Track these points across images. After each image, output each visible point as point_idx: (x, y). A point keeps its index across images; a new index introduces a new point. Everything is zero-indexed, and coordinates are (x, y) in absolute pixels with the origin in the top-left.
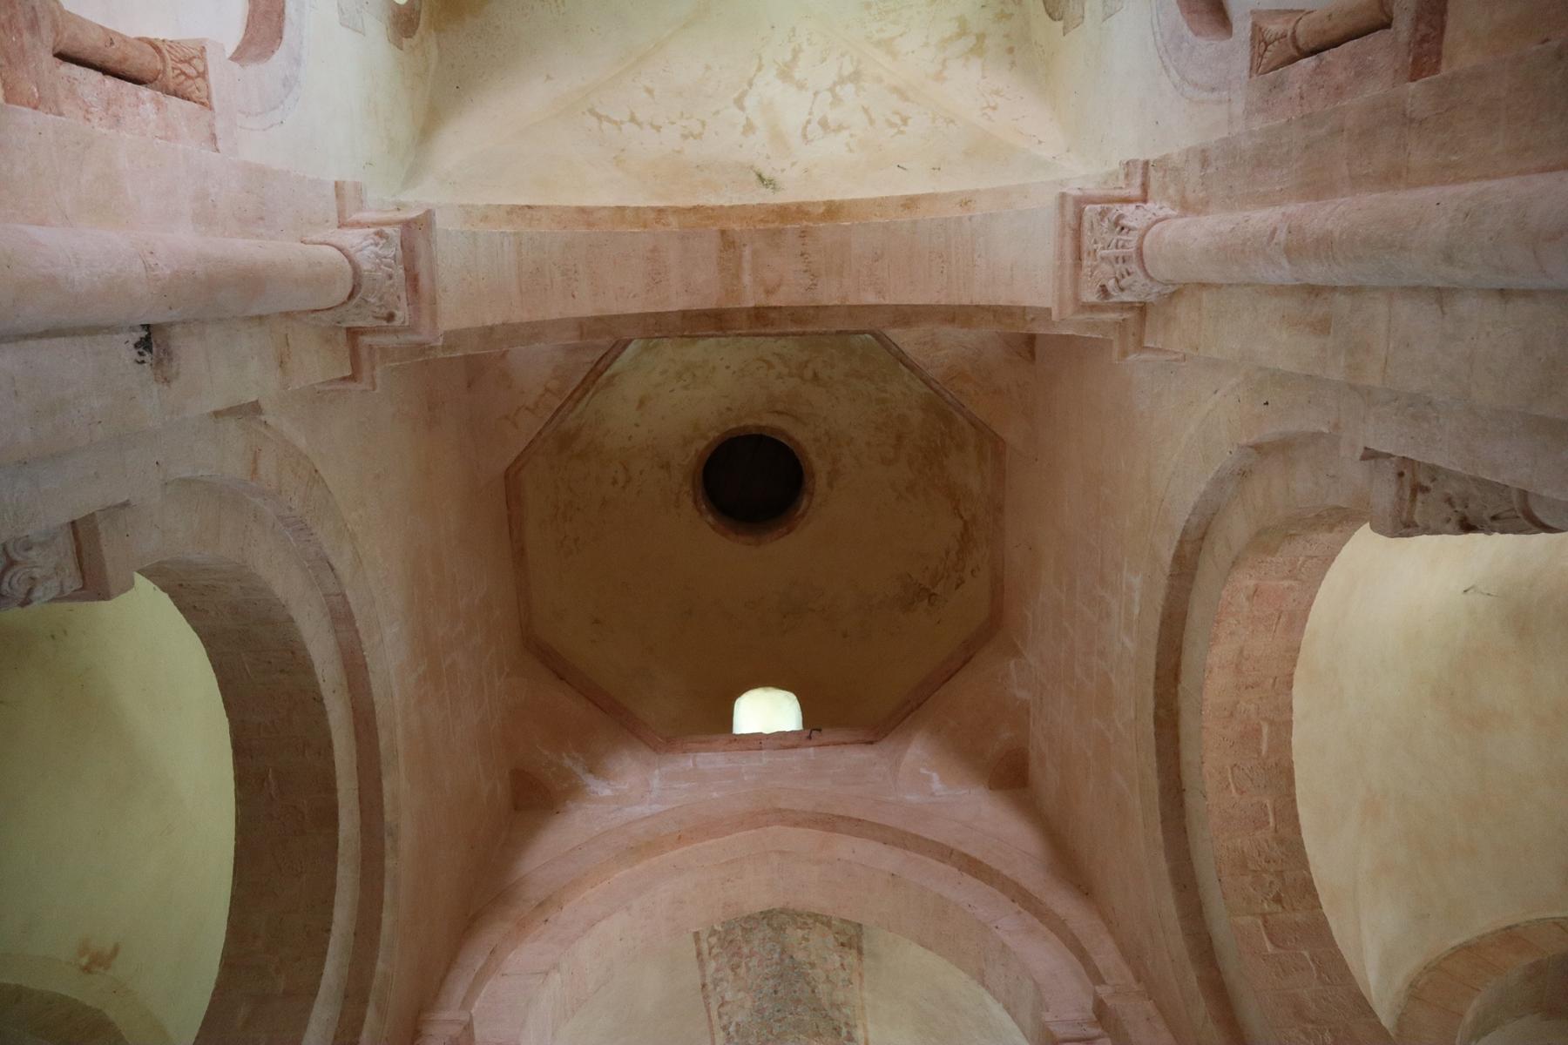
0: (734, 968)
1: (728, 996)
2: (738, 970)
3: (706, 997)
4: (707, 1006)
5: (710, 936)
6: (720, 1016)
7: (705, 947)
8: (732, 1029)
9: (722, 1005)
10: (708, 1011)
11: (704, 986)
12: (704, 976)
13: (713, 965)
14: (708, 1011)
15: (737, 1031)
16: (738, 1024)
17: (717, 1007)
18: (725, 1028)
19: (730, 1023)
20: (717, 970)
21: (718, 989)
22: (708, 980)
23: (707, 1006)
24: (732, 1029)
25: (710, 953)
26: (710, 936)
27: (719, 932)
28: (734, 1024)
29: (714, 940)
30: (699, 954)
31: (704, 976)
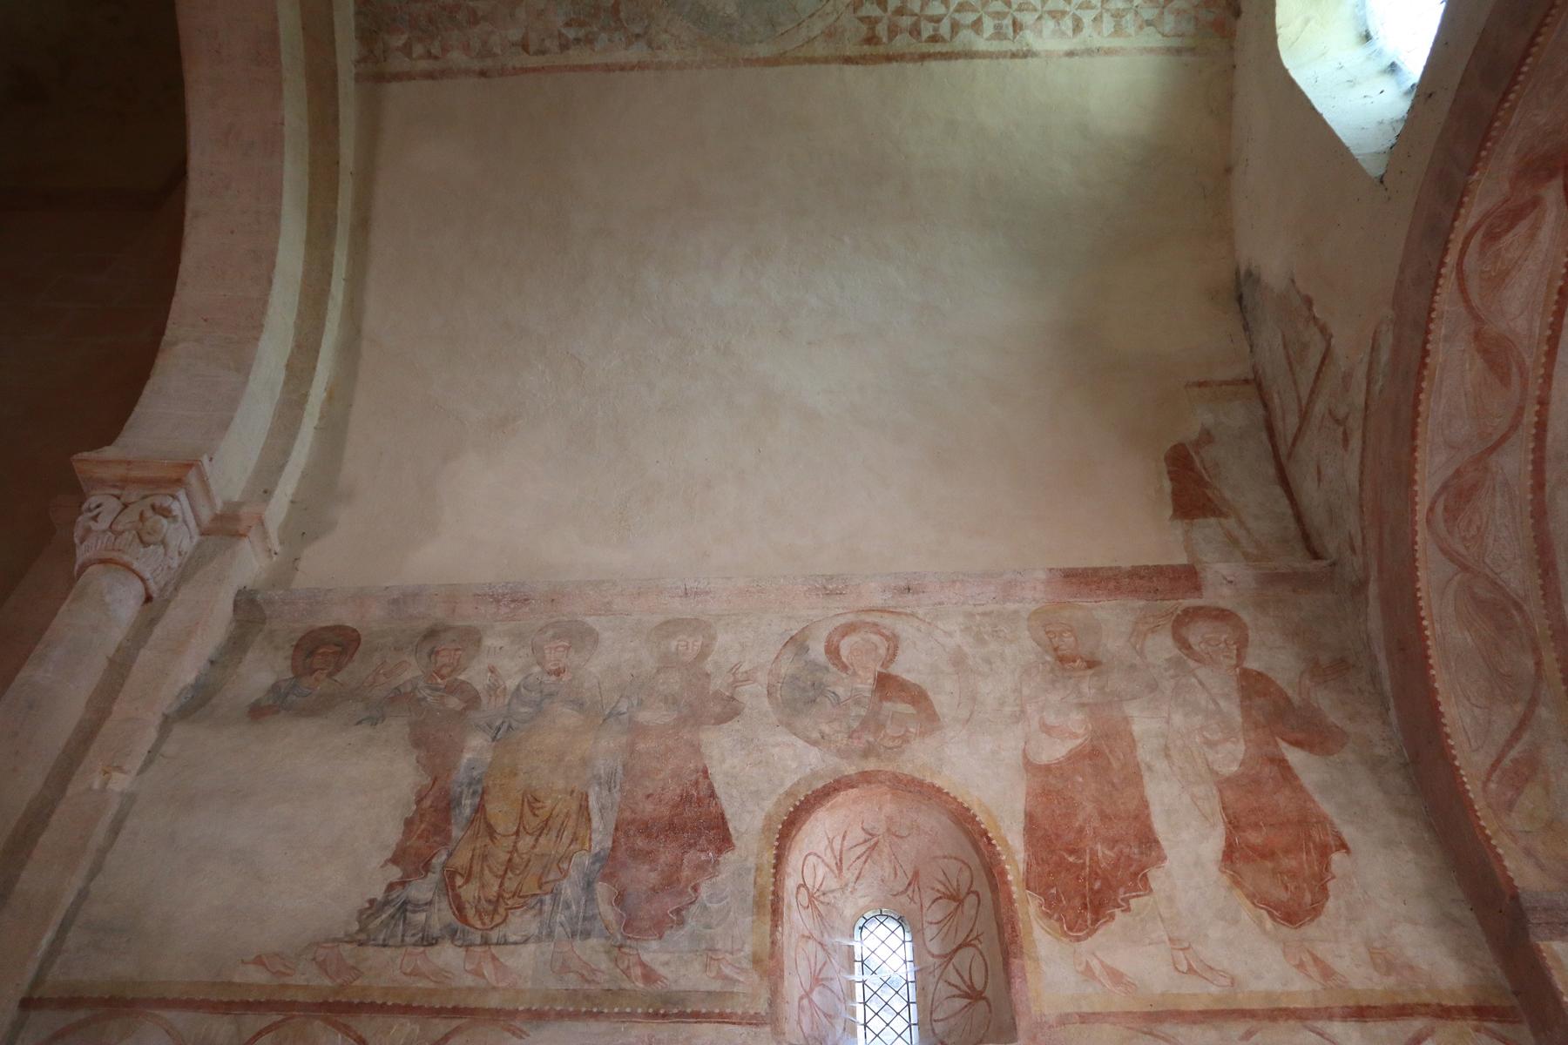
0: (474, 18)
1: (515, 34)
2: (480, 14)
3: (503, 72)
4: (517, 71)
5: (409, 55)
6: (543, 52)
7: (423, 65)
8: (571, 34)
9: (525, 48)
10: (525, 70)
11: (483, 74)
12: (467, 72)
13: (457, 57)
14: (525, 70)
15: (581, 25)
16: (568, 25)
17: (525, 55)
18: (564, 46)
19: (560, 35)
20: (467, 48)
21: (498, 50)
22: (477, 65)
23: (517, 71)
24: (571, 34)
25: (436, 58)
26: (409, 55)
27: (409, 38)
28: (564, 31)
29: (418, 49)
30: (430, 75)
31: (467, 72)
